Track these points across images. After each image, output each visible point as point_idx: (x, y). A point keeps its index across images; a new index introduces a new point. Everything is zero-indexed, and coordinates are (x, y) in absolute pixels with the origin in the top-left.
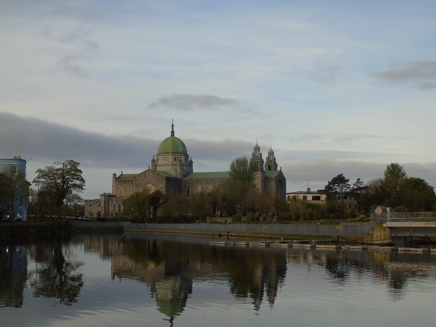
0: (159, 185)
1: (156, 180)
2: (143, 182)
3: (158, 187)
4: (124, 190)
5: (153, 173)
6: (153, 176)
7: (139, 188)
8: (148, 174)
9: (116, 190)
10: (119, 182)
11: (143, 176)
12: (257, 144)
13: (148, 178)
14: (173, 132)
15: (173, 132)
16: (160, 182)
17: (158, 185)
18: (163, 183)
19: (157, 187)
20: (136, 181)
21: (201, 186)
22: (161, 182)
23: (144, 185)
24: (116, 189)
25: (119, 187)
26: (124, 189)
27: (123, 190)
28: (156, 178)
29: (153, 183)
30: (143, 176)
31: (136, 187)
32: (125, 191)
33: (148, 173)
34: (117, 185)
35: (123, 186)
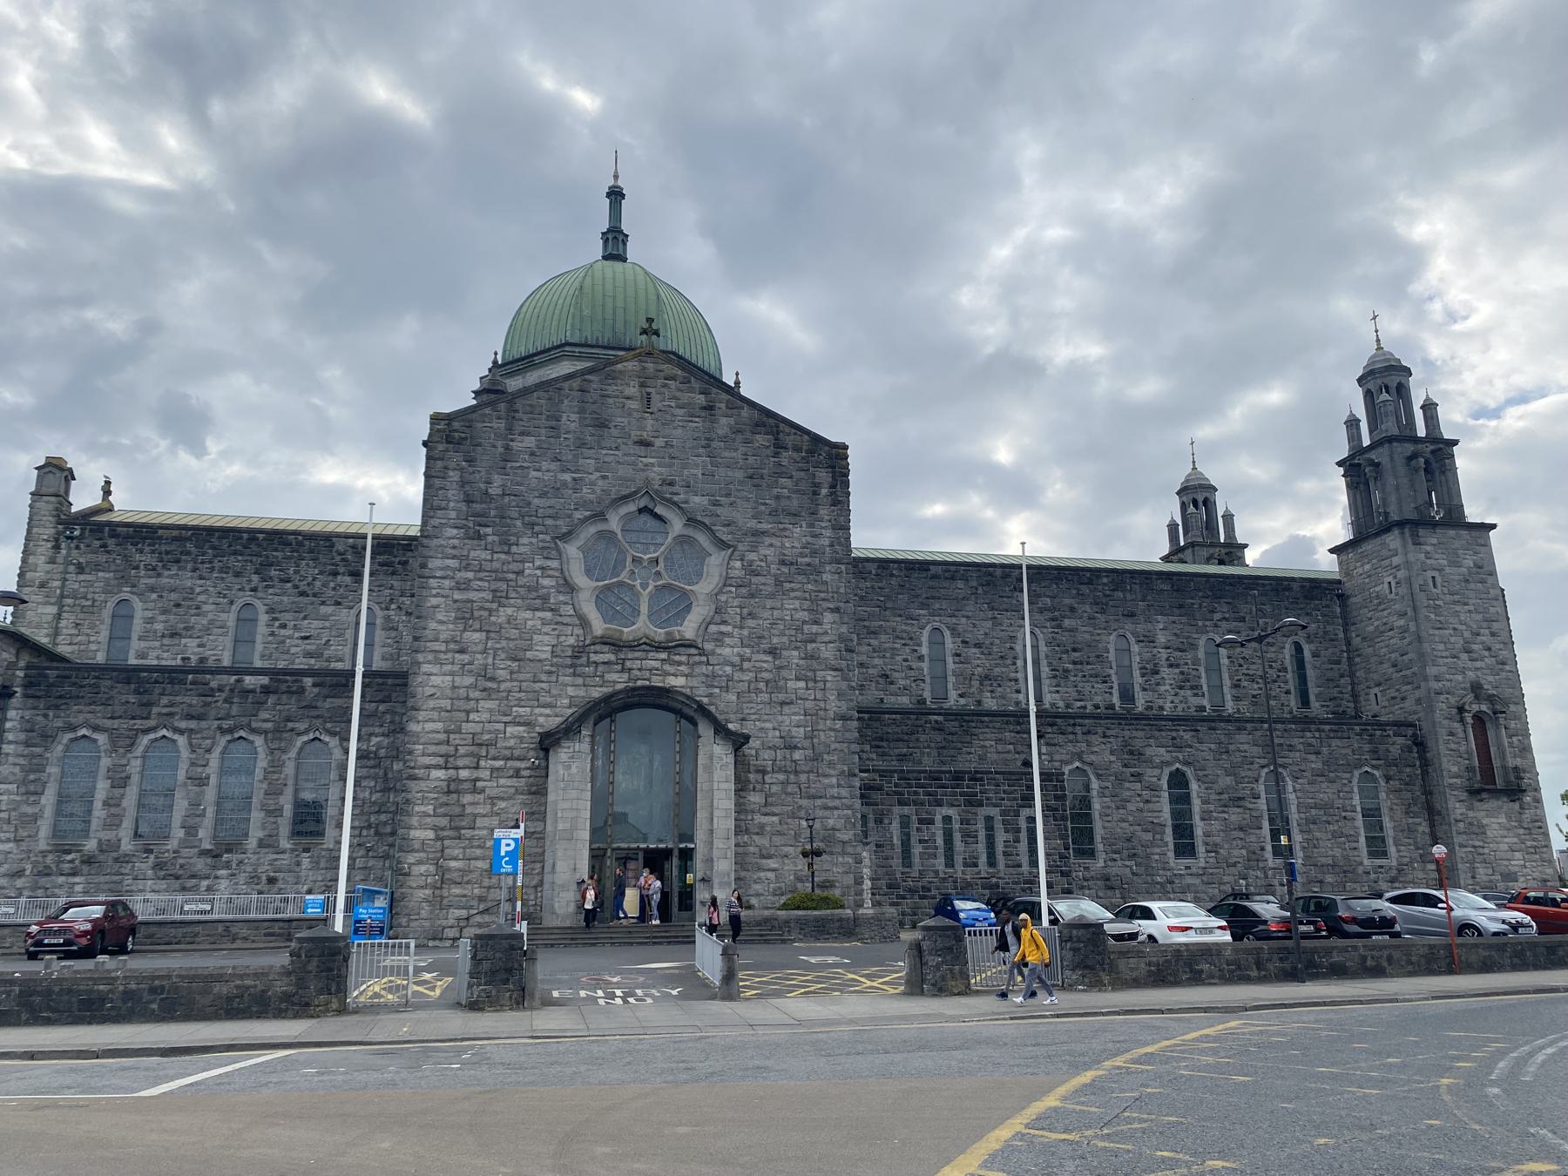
0: (765, 526)
1: (739, 475)
2: (567, 477)
3: (764, 551)
4: (159, 627)
5: (701, 399)
6: (698, 423)
7: (506, 543)
8: (633, 405)
9: (58, 617)
10: (111, 542)
11: (570, 420)
12: (1379, 348)
13: (641, 450)
14: (615, 242)
15: (615, 242)
16: (784, 503)
17: (757, 533)
18: (823, 512)
19: (753, 549)
20: (470, 461)
21: (953, 630)
22: (794, 503)
23: (578, 515)
24: (53, 610)
25: (100, 598)
26: (165, 612)
27: (150, 621)
28: (738, 455)
29: (697, 501)
30: (570, 420)
31: (479, 537)
32: (172, 635)
33: (633, 390)
34: (81, 569)
35: (152, 589)
